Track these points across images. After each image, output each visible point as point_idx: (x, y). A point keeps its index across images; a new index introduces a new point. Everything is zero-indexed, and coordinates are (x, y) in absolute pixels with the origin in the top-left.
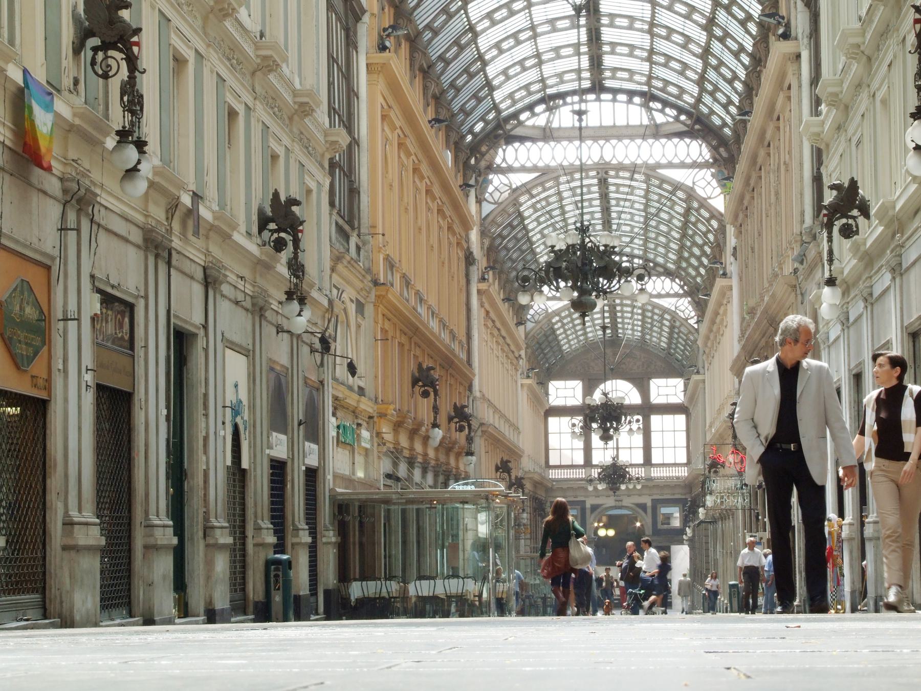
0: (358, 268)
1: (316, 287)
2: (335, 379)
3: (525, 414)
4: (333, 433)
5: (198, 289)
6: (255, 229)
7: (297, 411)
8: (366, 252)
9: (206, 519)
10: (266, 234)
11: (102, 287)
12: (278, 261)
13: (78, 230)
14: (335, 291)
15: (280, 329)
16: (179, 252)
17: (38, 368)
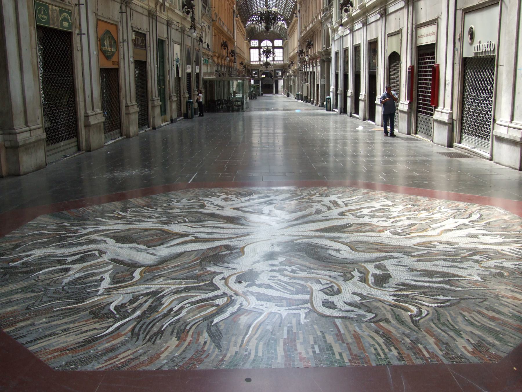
2: (203, 48)
3: (246, 49)
4: (203, 62)
5: (165, 27)
6: (181, 8)
7: (193, 58)
9: (170, 94)
10: (184, 9)
11: (135, 30)
12: (187, 17)
13: (126, 13)
15: (189, 36)
16: (159, 17)
17: (114, 59)
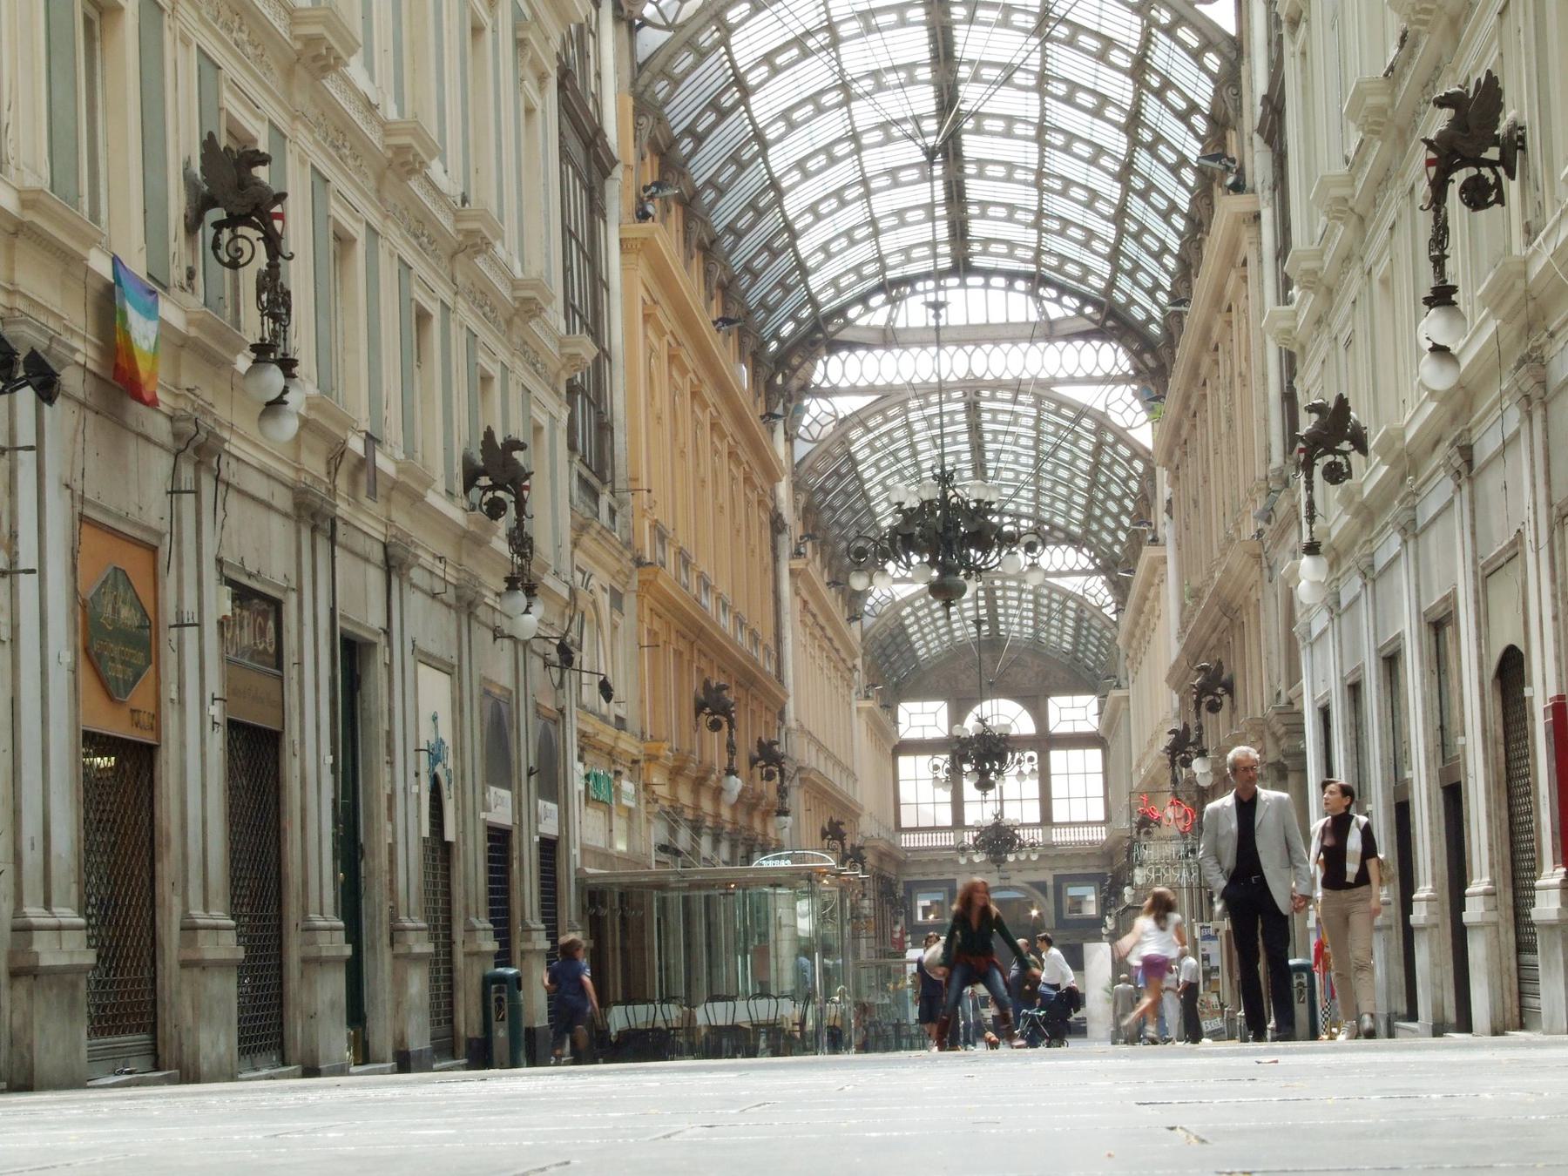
0: (613, 540)
1: (552, 571)
8: (624, 516)
14: (579, 576)
